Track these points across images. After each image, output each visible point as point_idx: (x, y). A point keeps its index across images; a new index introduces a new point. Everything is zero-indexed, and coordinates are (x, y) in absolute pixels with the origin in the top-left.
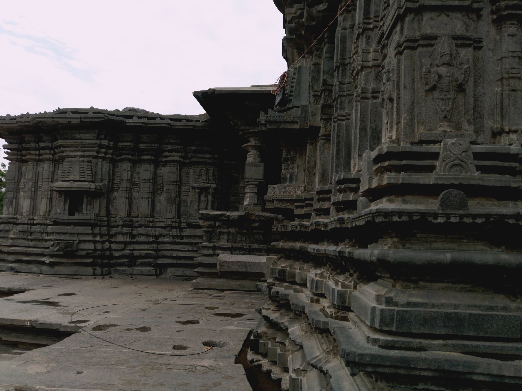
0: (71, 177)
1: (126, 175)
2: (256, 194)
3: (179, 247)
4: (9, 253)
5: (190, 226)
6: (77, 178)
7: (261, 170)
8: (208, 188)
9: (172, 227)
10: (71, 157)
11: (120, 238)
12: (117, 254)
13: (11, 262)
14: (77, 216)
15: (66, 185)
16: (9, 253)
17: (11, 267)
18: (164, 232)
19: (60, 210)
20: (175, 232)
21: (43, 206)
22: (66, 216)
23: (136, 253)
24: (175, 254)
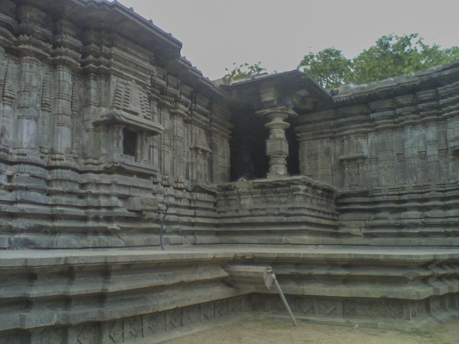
0: (132, 108)
2: (286, 166)
3: (192, 212)
6: (138, 109)
10: (121, 76)
13: (22, 231)
17: (27, 240)
18: (180, 193)
20: (188, 195)
21: (64, 141)
24: (193, 220)
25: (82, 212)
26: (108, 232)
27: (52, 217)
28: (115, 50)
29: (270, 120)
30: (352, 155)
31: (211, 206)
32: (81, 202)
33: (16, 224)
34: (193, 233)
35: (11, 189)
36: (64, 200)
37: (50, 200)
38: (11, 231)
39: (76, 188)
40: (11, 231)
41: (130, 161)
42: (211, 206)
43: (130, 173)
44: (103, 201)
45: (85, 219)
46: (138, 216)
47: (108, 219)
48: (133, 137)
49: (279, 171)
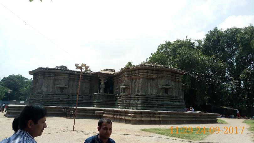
0: (61, 84)
1: (72, 84)
3: (82, 100)
4: (42, 101)
5: (84, 96)
6: (63, 84)
7: (104, 86)
8: (88, 88)
9: (81, 96)
11: (71, 98)
12: (70, 101)
14: (63, 93)
15: (61, 86)
16: (42, 101)
19: (58, 91)
20: (81, 97)
21: (51, 91)
22: (61, 93)
23: (74, 101)
24: (82, 101)
25: (52, 101)
26: (56, 104)
27: (48, 101)
28: (59, 76)
29: (101, 80)
30: (118, 87)
31: (89, 99)
32: (53, 99)
33: (42, 102)
34: (82, 104)
35: (42, 98)
36: (49, 99)
37: (47, 99)
38: (42, 103)
39: (52, 97)
40: (42, 103)
41: (61, 93)
42: (89, 99)
43: (60, 95)
44: (55, 99)
45: (53, 102)
46: (61, 101)
47: (56, 102)
48: (62, 89)
49: (102, 91)
